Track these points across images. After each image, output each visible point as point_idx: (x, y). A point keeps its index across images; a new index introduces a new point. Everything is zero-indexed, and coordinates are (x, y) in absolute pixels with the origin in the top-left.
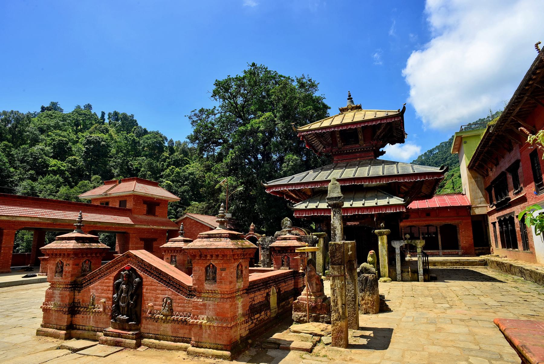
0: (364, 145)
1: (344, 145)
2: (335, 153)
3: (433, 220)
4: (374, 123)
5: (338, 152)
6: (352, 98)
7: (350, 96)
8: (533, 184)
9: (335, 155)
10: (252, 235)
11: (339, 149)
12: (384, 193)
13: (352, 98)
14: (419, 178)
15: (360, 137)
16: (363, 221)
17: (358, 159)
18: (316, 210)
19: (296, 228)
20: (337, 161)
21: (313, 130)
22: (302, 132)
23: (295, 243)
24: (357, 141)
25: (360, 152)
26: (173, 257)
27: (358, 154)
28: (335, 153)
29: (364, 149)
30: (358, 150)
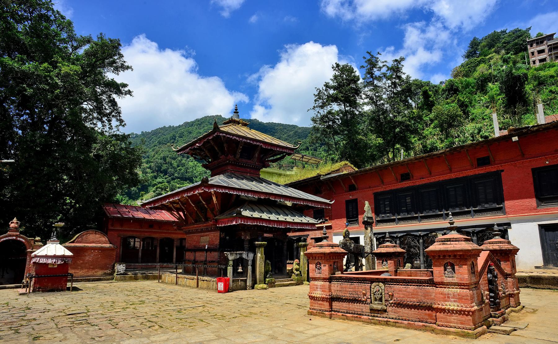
0: (257, 163)
1: (240, 157)
2: (232, 162)
3: (157, 232)
4: (278, 149)
5: (234, 163)
6: (238, 113)
7: (236, 110)
8: (345, 219)
9: (231, 164)
10: (14, 238)
11: (238, 160)
12: (296, 213)
13: (238, 113)
14: (319, 205)
15: (256, 155)
16: (276, 234)
17: (248, 174)
18: (260, 219)
19: (96, 232)
20: (231, 170)
21: (225, 133)
22: (221, 133)
23: (399, 250)
24: (250, 157)
25: (250, 168)
26: (336, 264)
27: (248, 170)
28: (232, 162)
29: (255, 166)
30: (250, 165)
